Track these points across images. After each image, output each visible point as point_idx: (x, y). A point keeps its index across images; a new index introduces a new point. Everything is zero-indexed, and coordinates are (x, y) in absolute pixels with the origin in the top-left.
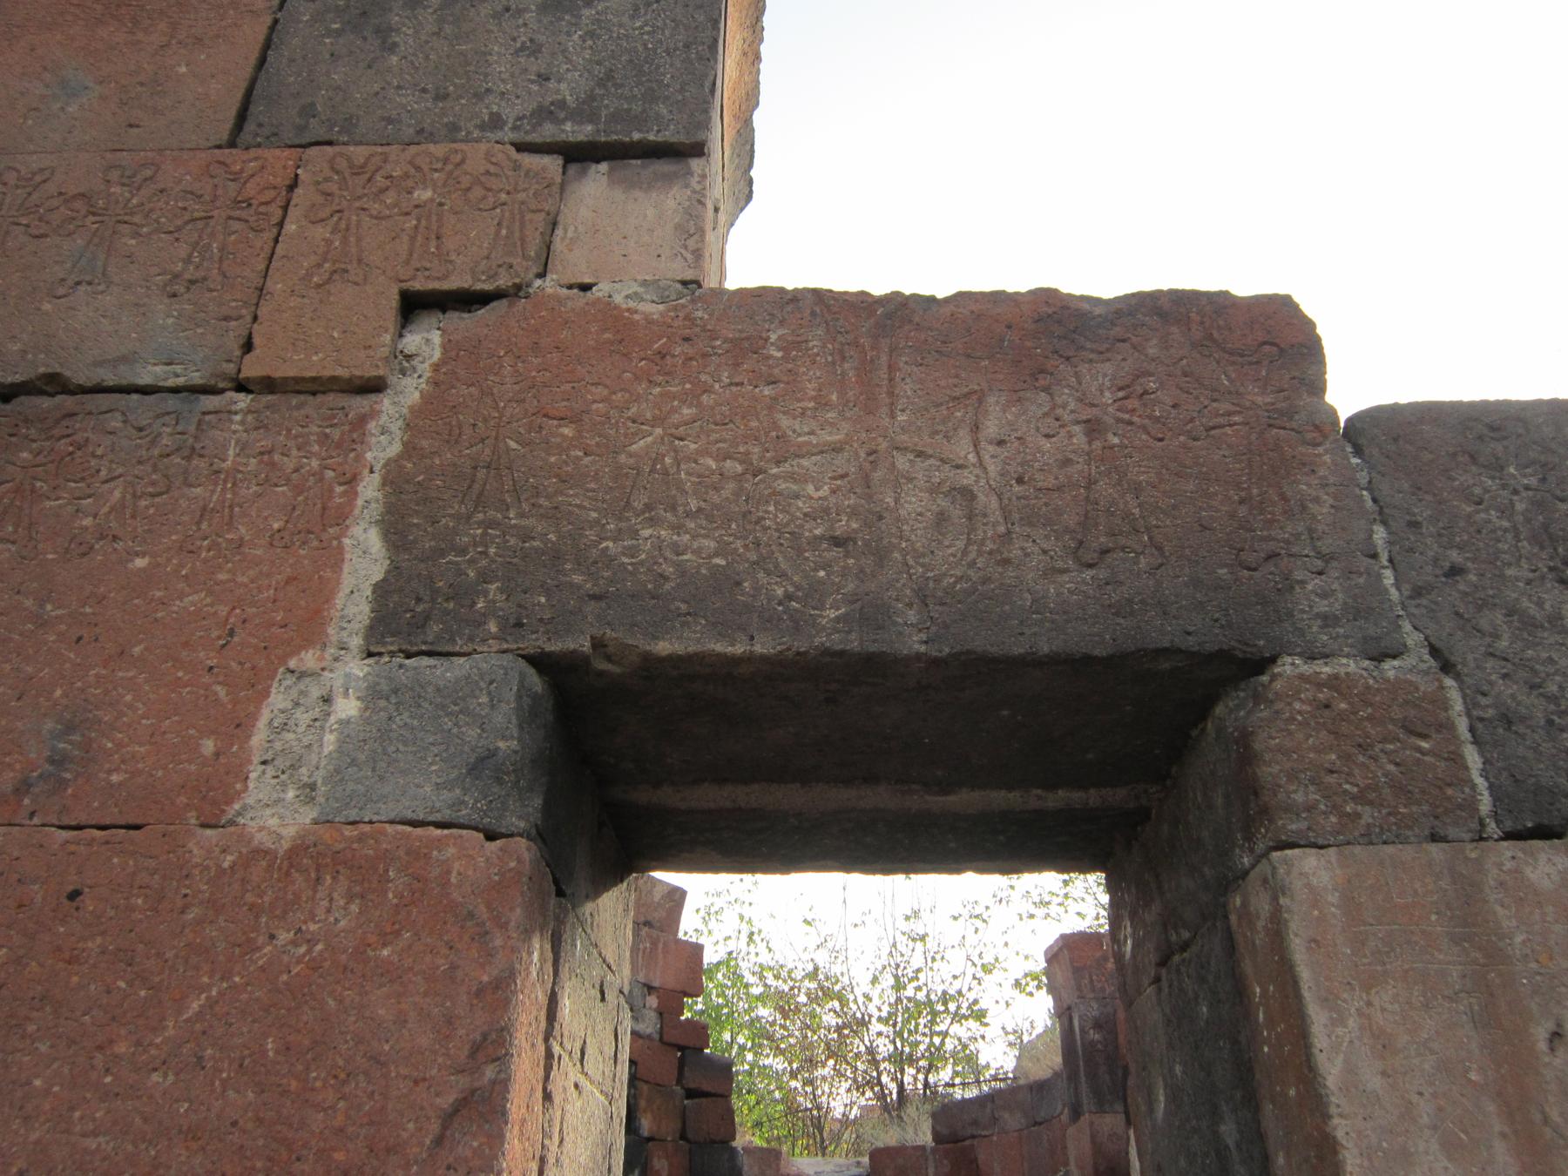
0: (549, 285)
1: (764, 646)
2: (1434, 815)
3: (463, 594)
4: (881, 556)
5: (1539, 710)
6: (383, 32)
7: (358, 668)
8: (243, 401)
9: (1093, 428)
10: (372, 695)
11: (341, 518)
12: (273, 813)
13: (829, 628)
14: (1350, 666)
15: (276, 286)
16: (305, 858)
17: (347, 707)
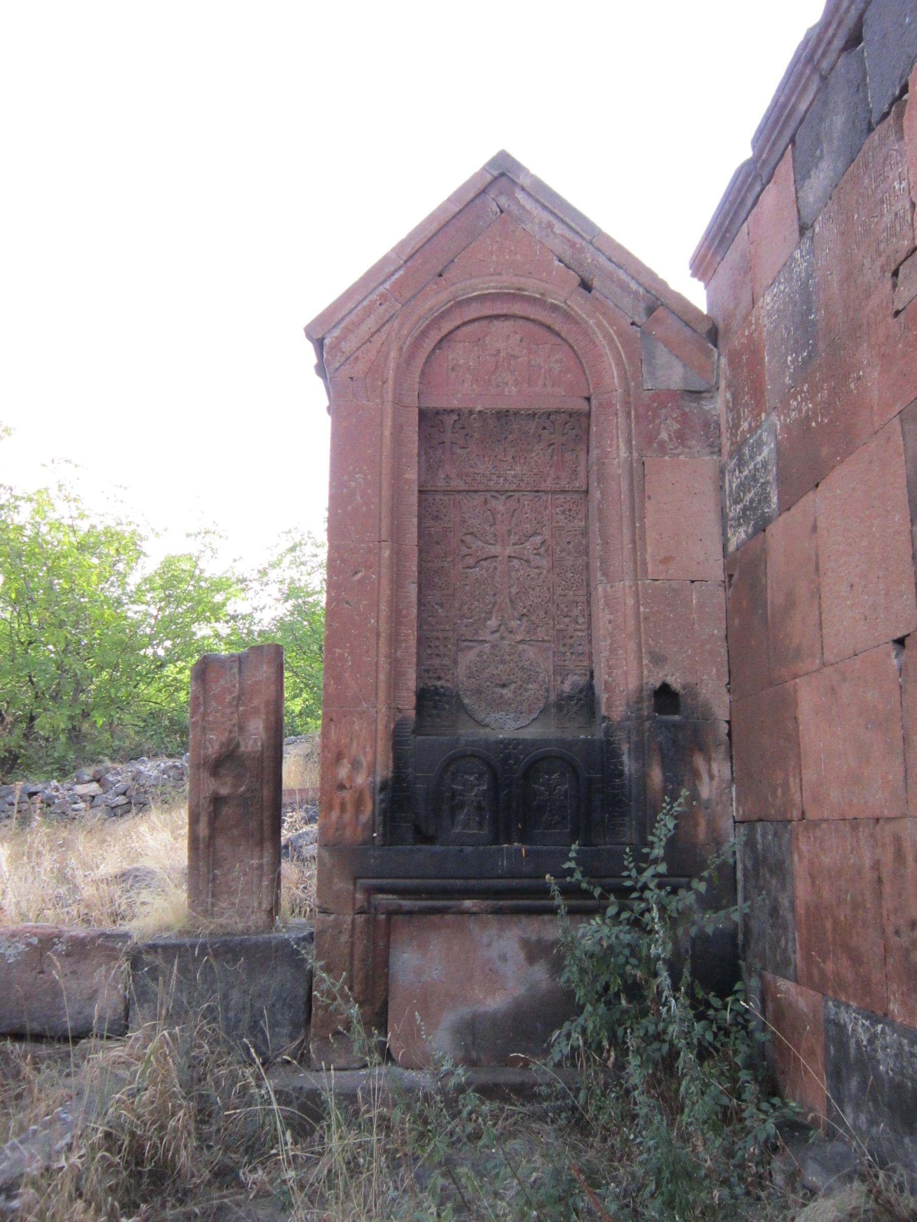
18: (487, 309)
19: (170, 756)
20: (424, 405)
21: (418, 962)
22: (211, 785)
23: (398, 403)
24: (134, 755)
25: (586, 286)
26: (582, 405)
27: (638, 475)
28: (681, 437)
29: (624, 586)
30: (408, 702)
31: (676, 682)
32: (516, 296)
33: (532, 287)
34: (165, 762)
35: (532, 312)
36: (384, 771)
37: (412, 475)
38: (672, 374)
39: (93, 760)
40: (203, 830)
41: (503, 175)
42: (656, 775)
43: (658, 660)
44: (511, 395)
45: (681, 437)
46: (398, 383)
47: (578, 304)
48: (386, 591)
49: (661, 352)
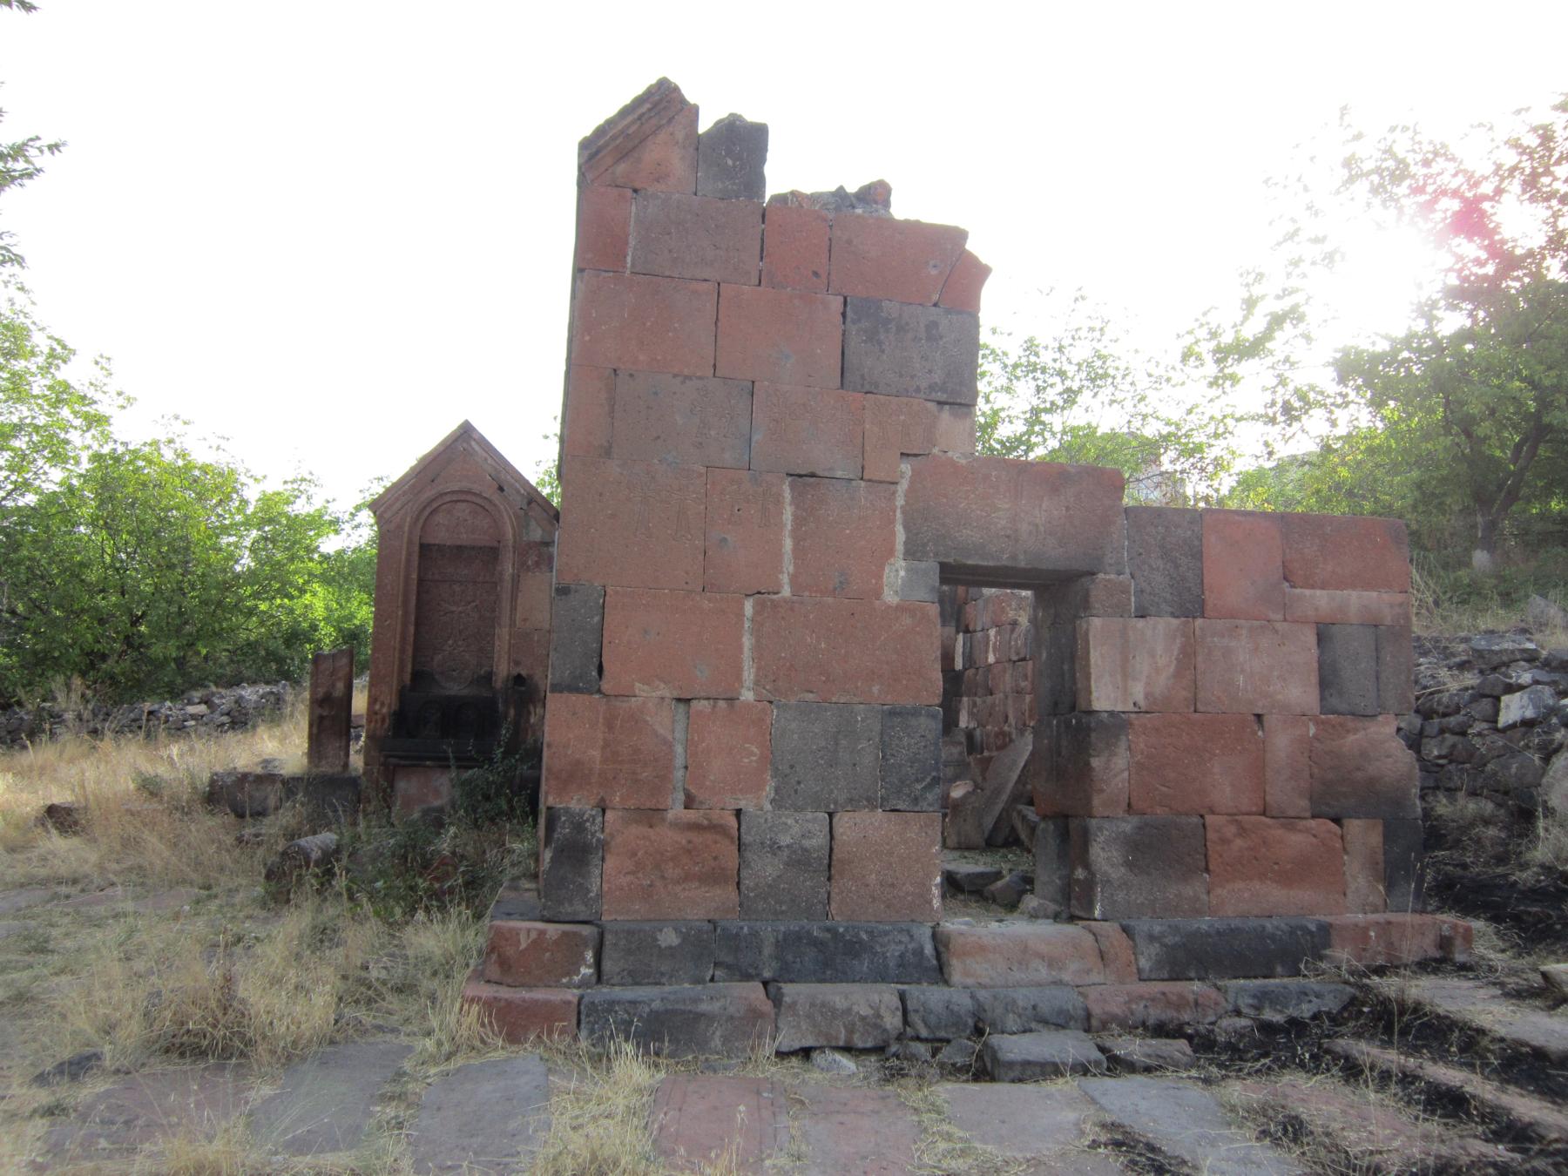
0: (935, 451)
1: (991, 563)
2: (1120, 611)
3: (924, 545)
4: (1017, 541)
5: (1148, 589)
6: (880, 343)
7: (903, 563)
8: (863, 484)
9: (1068, 508)
10: (907, 570)
11: (892, 522)
12: (890, 597)
13: (1005, 560)
14: (1112, 576)
15: (867, 448)
16: (900, 609)
17: (902, 573)
18: (455, 498)
19: (267, 683)
20: (425, 541)
21: (406, 786)
22: (319, 711)
23: (410, 542)
24: (235, 682)
25: (501, 489)
26: (495, 544)
27: (516, 581)
28: (537, 564)
29: (505, 630)
30: (407, 678)
31: (524, 673)
32: (469, 492)
33: (476, 488)
34: (263, 689)
35: (474, 499)
36: (395, 707)
37: (414, 576)
38: (537, 534)
39: (199, 684)
40: (315, 730)
41: (466, 433)
42: (512, 712)
43: (517, 663)
44: (465, 538)
45: (537, 564)
46: (411, 532)
47: (496, 498)
48: (399, 627)
49: (533, 523)
